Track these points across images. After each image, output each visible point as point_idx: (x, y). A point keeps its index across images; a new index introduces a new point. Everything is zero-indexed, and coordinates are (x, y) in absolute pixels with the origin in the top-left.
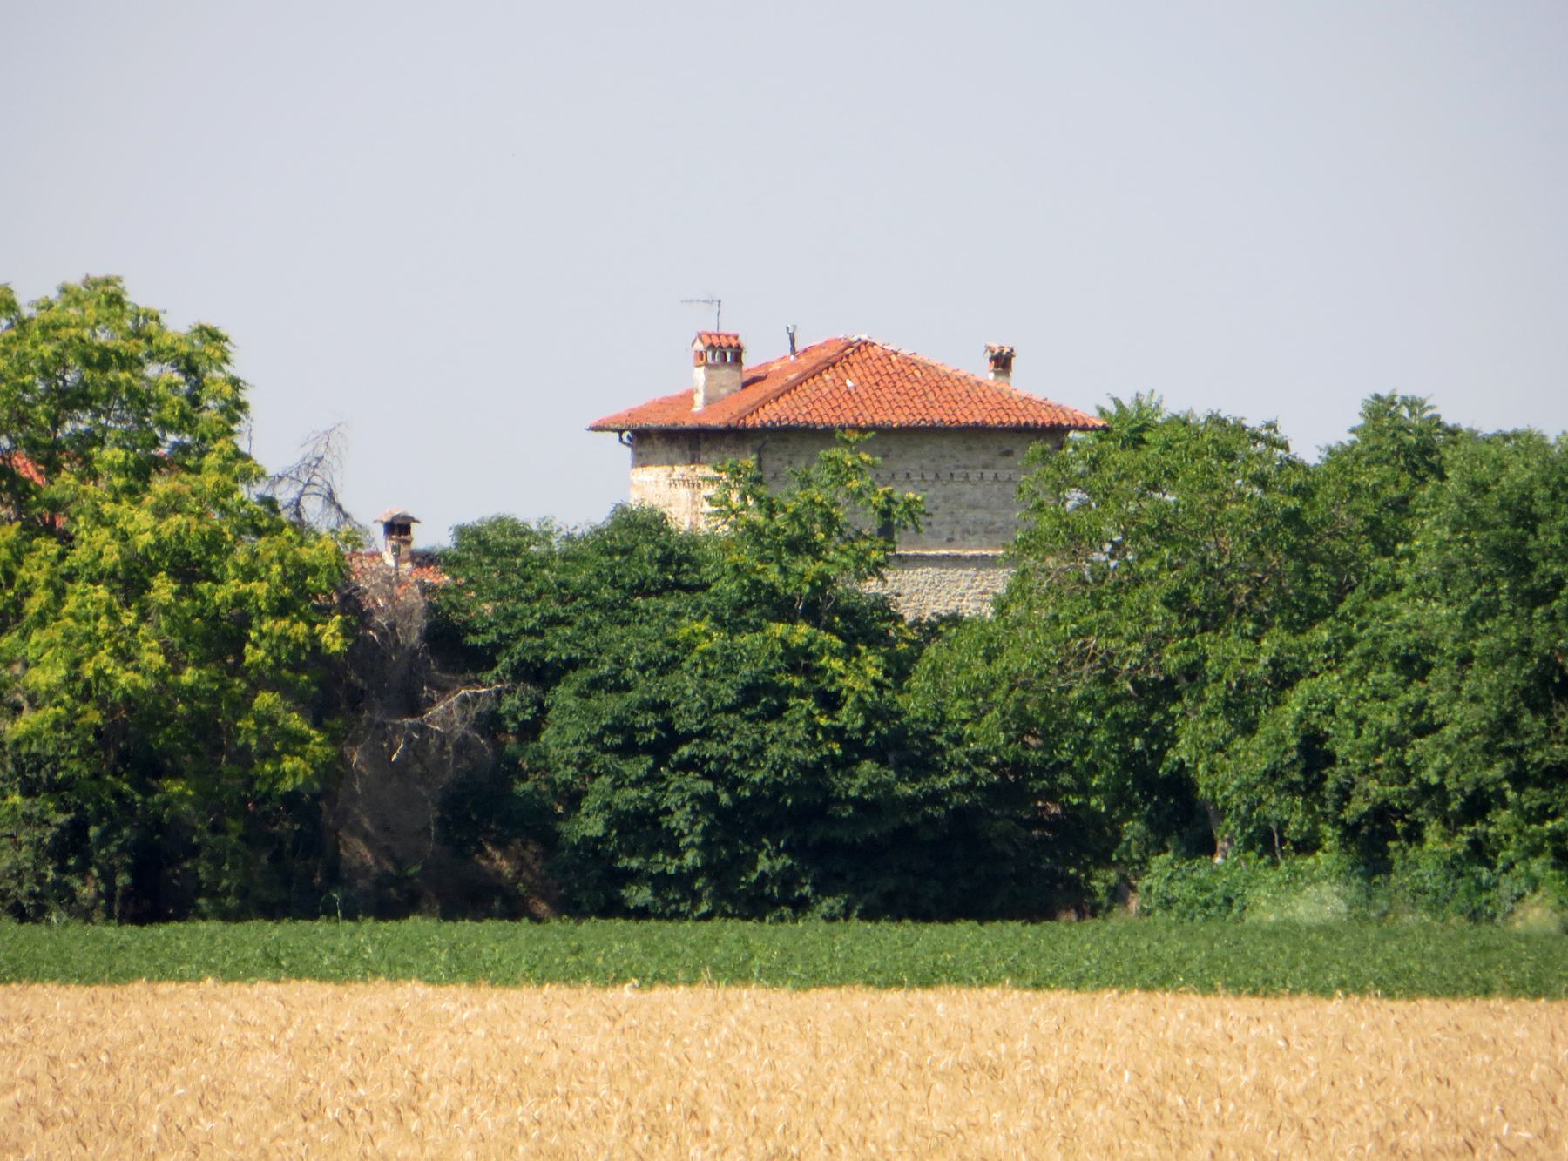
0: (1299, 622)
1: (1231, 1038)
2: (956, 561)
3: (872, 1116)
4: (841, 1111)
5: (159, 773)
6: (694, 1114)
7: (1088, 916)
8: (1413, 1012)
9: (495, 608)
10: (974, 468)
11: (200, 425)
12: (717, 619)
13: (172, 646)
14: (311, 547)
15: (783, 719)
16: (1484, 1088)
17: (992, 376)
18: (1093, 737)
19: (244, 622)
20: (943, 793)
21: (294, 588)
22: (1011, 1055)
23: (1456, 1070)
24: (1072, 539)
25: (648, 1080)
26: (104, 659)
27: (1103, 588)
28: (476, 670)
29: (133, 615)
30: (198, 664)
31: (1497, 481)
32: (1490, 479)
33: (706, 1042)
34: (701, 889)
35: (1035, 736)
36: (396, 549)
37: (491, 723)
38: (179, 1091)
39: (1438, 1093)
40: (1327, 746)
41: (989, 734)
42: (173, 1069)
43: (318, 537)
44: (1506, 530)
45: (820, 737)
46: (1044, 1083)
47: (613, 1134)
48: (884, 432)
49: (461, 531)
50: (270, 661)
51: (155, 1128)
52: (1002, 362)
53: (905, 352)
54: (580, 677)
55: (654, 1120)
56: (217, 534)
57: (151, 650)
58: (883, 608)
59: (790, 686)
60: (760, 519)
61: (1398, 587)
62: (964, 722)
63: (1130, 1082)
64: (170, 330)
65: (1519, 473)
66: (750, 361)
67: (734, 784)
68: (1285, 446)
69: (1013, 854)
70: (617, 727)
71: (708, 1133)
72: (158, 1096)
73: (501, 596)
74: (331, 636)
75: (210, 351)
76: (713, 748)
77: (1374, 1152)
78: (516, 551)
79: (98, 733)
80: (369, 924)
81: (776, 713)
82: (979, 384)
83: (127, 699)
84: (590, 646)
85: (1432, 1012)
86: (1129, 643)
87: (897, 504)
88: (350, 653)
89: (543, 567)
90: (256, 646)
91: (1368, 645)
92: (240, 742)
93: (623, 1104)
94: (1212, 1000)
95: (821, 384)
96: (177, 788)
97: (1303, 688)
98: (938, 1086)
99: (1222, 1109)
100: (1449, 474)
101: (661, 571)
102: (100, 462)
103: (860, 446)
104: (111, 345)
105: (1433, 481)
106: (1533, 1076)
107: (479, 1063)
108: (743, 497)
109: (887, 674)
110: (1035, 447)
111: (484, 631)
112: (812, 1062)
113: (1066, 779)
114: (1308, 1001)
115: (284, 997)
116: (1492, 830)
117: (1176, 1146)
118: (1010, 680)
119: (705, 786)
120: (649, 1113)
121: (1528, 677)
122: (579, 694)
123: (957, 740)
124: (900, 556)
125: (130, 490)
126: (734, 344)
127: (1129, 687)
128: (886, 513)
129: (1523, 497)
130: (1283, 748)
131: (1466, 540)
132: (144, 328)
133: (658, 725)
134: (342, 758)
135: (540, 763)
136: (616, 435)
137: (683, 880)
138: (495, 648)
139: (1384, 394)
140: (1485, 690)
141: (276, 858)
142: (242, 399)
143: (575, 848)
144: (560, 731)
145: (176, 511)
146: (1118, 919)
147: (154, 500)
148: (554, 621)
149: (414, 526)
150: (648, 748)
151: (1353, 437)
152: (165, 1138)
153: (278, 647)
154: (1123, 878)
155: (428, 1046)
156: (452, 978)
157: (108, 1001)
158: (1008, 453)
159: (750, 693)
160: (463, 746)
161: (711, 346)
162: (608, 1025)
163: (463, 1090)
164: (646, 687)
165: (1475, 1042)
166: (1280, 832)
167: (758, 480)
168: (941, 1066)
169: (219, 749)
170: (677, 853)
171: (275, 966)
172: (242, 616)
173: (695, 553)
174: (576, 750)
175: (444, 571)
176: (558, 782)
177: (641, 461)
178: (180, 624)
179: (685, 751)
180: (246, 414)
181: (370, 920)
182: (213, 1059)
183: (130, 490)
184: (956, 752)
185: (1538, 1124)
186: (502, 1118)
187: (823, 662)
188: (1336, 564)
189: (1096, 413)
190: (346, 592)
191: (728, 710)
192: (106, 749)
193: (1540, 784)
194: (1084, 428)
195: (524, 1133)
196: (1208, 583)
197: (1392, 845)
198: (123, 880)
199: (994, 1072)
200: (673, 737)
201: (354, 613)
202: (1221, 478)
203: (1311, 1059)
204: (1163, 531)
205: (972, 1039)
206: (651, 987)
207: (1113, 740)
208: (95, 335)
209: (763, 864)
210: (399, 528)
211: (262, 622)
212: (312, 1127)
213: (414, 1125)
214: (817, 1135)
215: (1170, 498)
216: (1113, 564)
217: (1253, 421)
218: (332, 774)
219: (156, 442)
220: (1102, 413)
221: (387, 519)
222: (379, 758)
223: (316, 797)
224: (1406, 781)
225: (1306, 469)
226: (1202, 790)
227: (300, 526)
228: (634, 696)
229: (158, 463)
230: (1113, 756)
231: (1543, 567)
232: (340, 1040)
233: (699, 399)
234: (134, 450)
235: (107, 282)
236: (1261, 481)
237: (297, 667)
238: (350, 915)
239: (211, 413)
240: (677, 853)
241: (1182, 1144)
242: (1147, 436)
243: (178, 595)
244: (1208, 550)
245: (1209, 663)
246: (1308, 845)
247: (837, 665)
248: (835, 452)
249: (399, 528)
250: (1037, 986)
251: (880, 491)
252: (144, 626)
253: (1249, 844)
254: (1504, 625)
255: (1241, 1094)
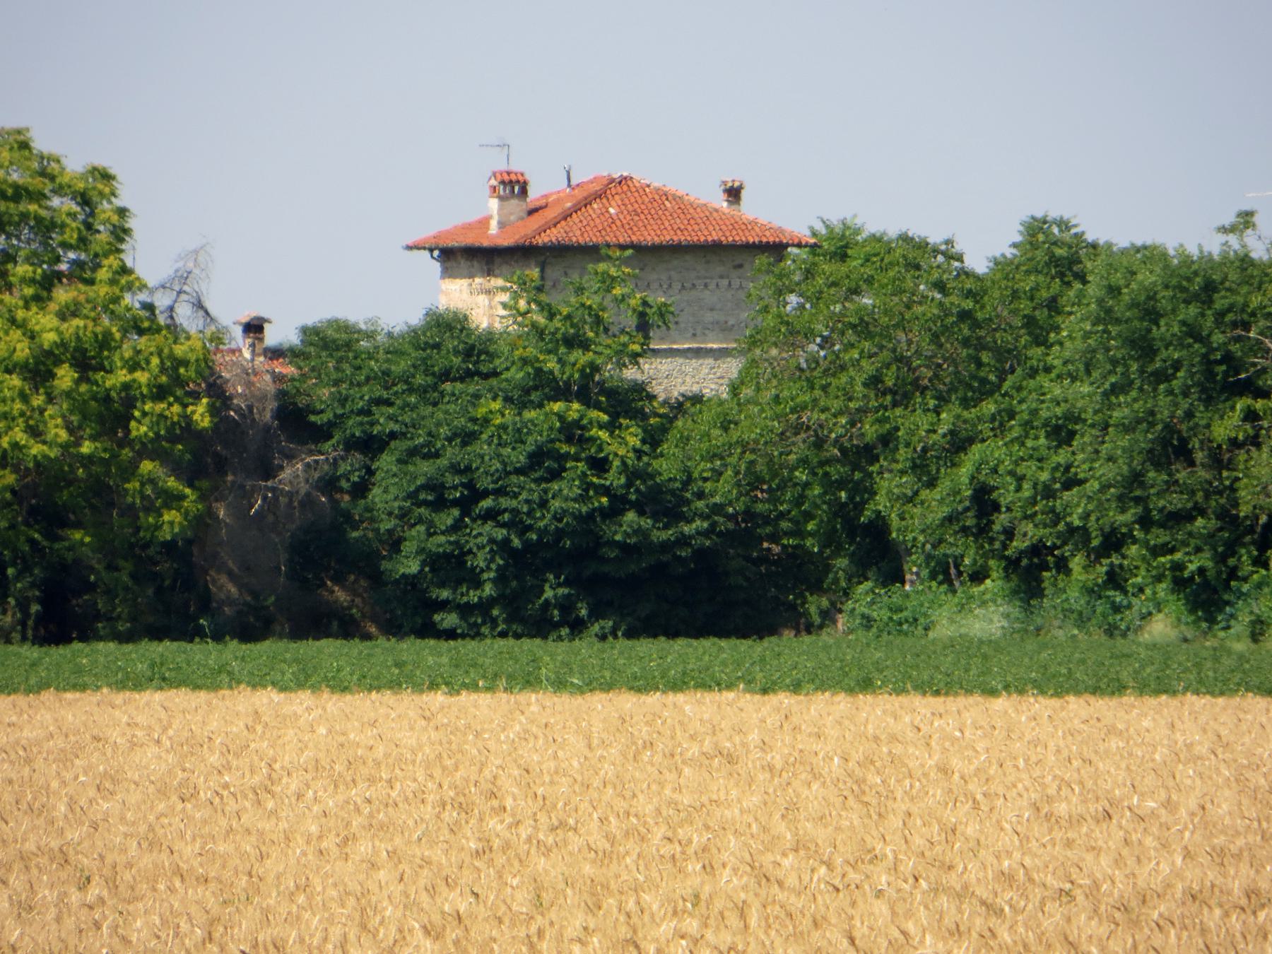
0: (972, 399)
1: (919, 730)
2: (698, 353)
3: (634, 796)
4: (610, 791)
5: (65, 524)
6: (494, 795)
7: (803, 633)
8: (1063, 708)
9: (331, 393)
10: (712, 278)
11: (93, 246)
12: (508, 399)
13: (72, 422)
14: (182, 344)
15: (563, 478)
16: (1118, 768)
17: (725, 204)
18: (808, 492)
19: (130, 403)
20: (691, 537)
21: (169, 376)
22: (744, 744)
23: (1096, 752)
24: (791, 333)
25: (457, 768)
26: (20, 436)
27: (815, 373)
28: (316, 442)
29: (42, 398)
30: (93, 438)
31: (1127, 286)
32: (1122, 282)
33: (502, 738)
34: (498, 617)
35: (762, 491)
36: (253, 346)
37: (329, 484)
38: (82, 778)
39: (1082, 771)
40: (995, 495)
41: (723, 490)
42: (77, 762)
43: (188, 338)
44: (1136, 323)
45: (591, 493)
46: (771, 768)
47: (428, 811)
48: (640, 249)
49: (305, 330)
50: (151, 434)
51: (63, 809)
52: (734, 193)
53: (656, 184)
54: (399, 446)
55: (462, 799)
56: (108, 335)
57: (57, 426)
58: (640, 390)
59: (568, 454)
60: (541, 320)
61: (1048, 370)
62: (705, 480)
63: (839, 766)
64: (68, 170)
65: (1147, 277)
66: (534, 193)
67: (526, 529)
68: (960, 258)
69: (745, 584)
70: (428, 486)
71: (505, 809)
72: (64, 783)
73: (336, 383)
74: (201, 414)
75: (100, 186)
76: (505, 502)
77: (1032, 819)
78: (348, 345)
79: (13, 492)
80: (233, 645)
81: (555, 475)
82: (717, 211)
83: (38, 464)
84: (408, 420)
85: (1076, 707)
86: (835, 416)
87: (651, 307)
88: (215, 428)
89: (370, 359)
90: (139, 422)
91: (1026, 416)
92: (130, 499)
93: (435, 786)
94: (903, 699)
95: (591, 212)
96: (78, 535)
97: (976, 451)
98: (687, 771)
99: (911, 786)
100: (1090, 278)
101: (464, 361)
102: (14, 275)
103: (626, 262)
104: (21, 182)
105: (1078, 285)
106: (1157, 757)
107: (321, 755)
108: (529, 303)
109: (644, 441)
110: (762, 260)
111: (322, 411)
112: (586, 752)
113: (785, 525)
114: (980, 699)
115: (166, 704)
116: (1126, 562)
117: (875, 817)
118: (743, 446)
119: (500, 534)
120: (457, 794)
121: (1152, 441)
122: (400, 461)
123: (700, 495)
124: (653, 350)
125: (37, 298)
126: (521, 178)
127: (836, 451)
128: (642, 315)
129: (1149, 298)
130: (958, 498)
131: (1104, 331)
132: (47, 170)
133: (463, 485)
134: (210, 513)
135: (368, 515)
136: (427, 253)
137: (484, 607)
138: (331, 424)
139: (1039, 214)
140: (1119, 452)
141: (159, 591)
142: (127, 226)
143: (397, 582)
144: (386, 491)
145: (74, 314)
146: (826, 637)
147: (57, 308)
148: (379, 402)
149: (266, 326)
150: (455, 503)
151: (1014, 251)
152: (70, 816)
153: (158, 424)
154: (833, 604)
155: (280, 742)
156: (301, 686)
157: (25, 707)
158: (740, 266)
159: (537, 457)
160: (308, 502)
161: (503, 182)
162: (423, 723)
163: (309, 776)
164: (452, 453)
165: (1111, 731)
166: (957, 566)
167: (540, 289)
168: (689, 754)
169: (112, 504)
170: (478, 584)
171: (162, 679)
172: (129, 396)
173: (492, 349)
174: (396, 504)
175: (290, 363)
176: (382, 531)
177: (447, 273)
178: (80, 407)
179: (487, 503)
180: (130, 236)
181: (235, 642)
182: (109, 752)
183: (37, 298)
184: (700, 504)
185: (1163, 795)
186: (340, 798)
187: (592, 433)
188: (1002, 354)
189: (808, 233)
190: (211, 380)
191: (519, 471)
192: (20, 504)
193: (1162, 525)
194: (799, 245)
195: (358, 810)
196: (898, 368)
197: (1046, 574)
198: (35, 608)
199: (731, 759)
200: (476, 494)
201: (218, 397)
202: (909, 284)
203: (980, 746)
204: (863, 327)
205: (714, 734)
206: (458, 693)
207: (825, 493)
208: (8, 174)
209: (549, 593)
210: (254, 328)
211: (144, 403)
212: (189, 806)
213: (270, 805)
214: (591, 810)
215: (867, 301)
216: (822, 353)
217: (935, 238)
218: (202, 524)
219: (58, 259)
220: (814, 234)
221: (245, 320)
222: (240, 512)
223: (189, 542)
224: (1056, 524)
225: (978, 278)
226: (894, 535)
227: (173, 329)
228: (443, 462)
229: (59, 276)
230: (825, 507)
231: (1164, 354)
232: (210, 739)
233: (494, 224)
234: (40, 266)
235: (19, 132)
236: (940, 286)
237: (173, 439)
238: (218, 637)
239: (103, 236)
240: (478, 584)
241: (880, 815)
242: (849, 252)
243: (78, 382)
244: (899, 342)
245: (900, 434)
246: (978, 576)
247: (603, 435)
248: (602, 267)
249: (254, 328)
250: (765, 691)
251: (638, 296)
252: (50, 407)
253: (933, 576)
254: (1135, 400)
255: (925, 775)
